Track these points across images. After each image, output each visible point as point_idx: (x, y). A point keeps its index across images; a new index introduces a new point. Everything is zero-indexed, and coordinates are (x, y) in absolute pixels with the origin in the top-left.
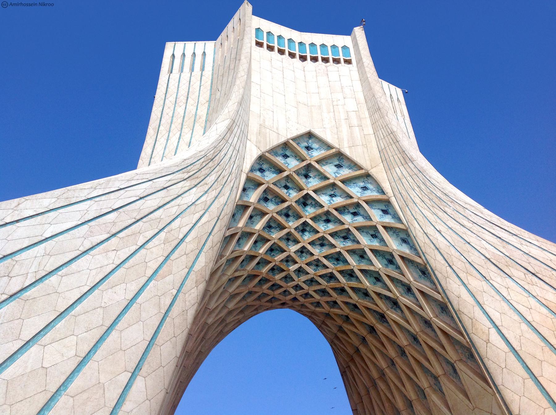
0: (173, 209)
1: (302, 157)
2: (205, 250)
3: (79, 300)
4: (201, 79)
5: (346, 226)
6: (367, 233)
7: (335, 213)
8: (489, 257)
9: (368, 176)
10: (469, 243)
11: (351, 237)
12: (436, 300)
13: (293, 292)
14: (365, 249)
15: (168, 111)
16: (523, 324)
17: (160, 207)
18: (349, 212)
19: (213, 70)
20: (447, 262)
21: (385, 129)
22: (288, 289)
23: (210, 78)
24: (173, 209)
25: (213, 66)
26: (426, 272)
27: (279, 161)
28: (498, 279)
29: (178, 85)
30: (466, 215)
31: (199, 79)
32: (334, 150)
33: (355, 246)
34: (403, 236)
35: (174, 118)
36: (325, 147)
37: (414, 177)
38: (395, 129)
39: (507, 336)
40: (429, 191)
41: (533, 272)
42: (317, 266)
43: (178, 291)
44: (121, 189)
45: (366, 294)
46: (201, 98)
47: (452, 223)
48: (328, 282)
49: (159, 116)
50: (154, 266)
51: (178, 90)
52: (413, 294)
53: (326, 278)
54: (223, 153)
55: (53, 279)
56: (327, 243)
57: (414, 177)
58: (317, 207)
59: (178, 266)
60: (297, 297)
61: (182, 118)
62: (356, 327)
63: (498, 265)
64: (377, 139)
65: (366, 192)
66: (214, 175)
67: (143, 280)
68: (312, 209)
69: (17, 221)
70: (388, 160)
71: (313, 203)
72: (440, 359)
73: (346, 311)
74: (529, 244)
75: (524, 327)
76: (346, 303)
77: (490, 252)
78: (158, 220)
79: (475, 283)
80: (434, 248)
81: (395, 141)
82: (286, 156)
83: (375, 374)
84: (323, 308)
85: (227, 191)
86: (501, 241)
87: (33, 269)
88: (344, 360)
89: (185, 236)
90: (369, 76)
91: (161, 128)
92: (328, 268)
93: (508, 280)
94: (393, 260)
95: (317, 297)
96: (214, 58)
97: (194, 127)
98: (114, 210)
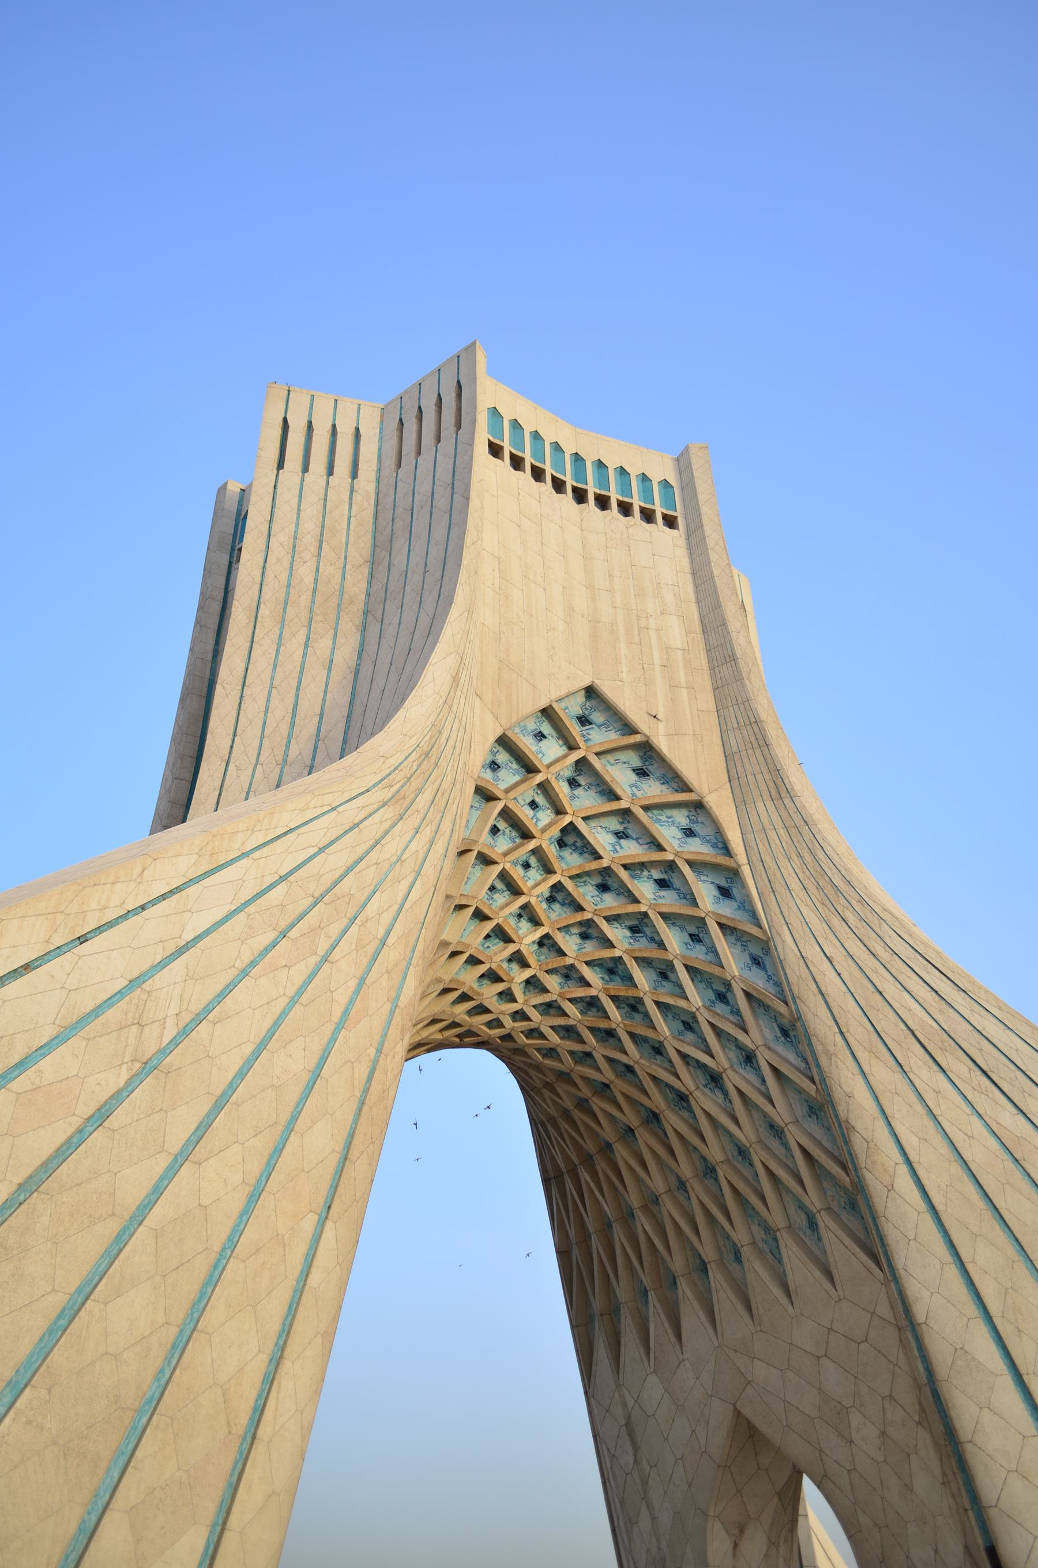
0: (370, 875)
1: (570, 740)
2: (414, 961)
3: (242, 1074)
4: (351, 498)
5: (643, 908)
6: (682, 929)
7: (624, 875)
8: (913, 1027)
9: (699, 806)
10: (880, 993)
11: (648, 931)
12: (801, 1091)
13: (508, 1022)
14: (675, 962)
15: (277, 570)
16: (953, 1163)
17: (350, 869)
18: (650, 877)
19: (378, 480)
20: (837, 1024)
21: (742, 706)
22: (500, 1017)
23: (373, 501)
24: (370, 875)
25: (379, 470)
26: (791, 1033)
28: (923, 1073)
29: (299, 505)
30: (881, 934)
31: (347, 499)
32: (637, 738)
33: (655, 954)
34: (757, 951)
35: (292, 591)
36: (618, 725)
37: (793, 831)
38: (763, 715)
39: (925, 1182)
40: (819, 869)
41: (985, 1068)
42: (567, 977)
44: (291, 831)
45: (658, 1050)
46: (352, 551)
48: (582, 1012)
49: (258, 579)
50: (342, 997)
51: (298, 518)
52: (757, 1069)
53: (580, 1005)
56: (596, 935)
57: (793, 831)
58: (586, 855)
60: (513, 1034)
61: (310, 593)
62: (619, 1108)
63: (926, 1044)
64: (724, 727)
65: (690, 840)
66: (430, 789)
68: (575, 855)
69: (143, 908)
70: (743, 780)
71: (579, 844)
72: (787, 1198)
73: (608, 1074)
74: (984, 1012)
75: (957, 1169)
76: (610, 1060)
77: (917, 1017)
78: (347, 899)
79: (883, 1074)
80: (816, 991)
81: (762, 743)
82: (540, 736)
83: (634, 1199)
84: (561, 1061)
86: (937, 998)
87: (173, 1010)
88: (567, 1158)
89: (388, 933)
90: (716, 572)
91: (264, 611)
92: (589, 985)
93: (941, 1076)
94: (729, 995)
95: (554, 1038)
96: (380, 449)
97: (337, 623)
98: (283, 878)
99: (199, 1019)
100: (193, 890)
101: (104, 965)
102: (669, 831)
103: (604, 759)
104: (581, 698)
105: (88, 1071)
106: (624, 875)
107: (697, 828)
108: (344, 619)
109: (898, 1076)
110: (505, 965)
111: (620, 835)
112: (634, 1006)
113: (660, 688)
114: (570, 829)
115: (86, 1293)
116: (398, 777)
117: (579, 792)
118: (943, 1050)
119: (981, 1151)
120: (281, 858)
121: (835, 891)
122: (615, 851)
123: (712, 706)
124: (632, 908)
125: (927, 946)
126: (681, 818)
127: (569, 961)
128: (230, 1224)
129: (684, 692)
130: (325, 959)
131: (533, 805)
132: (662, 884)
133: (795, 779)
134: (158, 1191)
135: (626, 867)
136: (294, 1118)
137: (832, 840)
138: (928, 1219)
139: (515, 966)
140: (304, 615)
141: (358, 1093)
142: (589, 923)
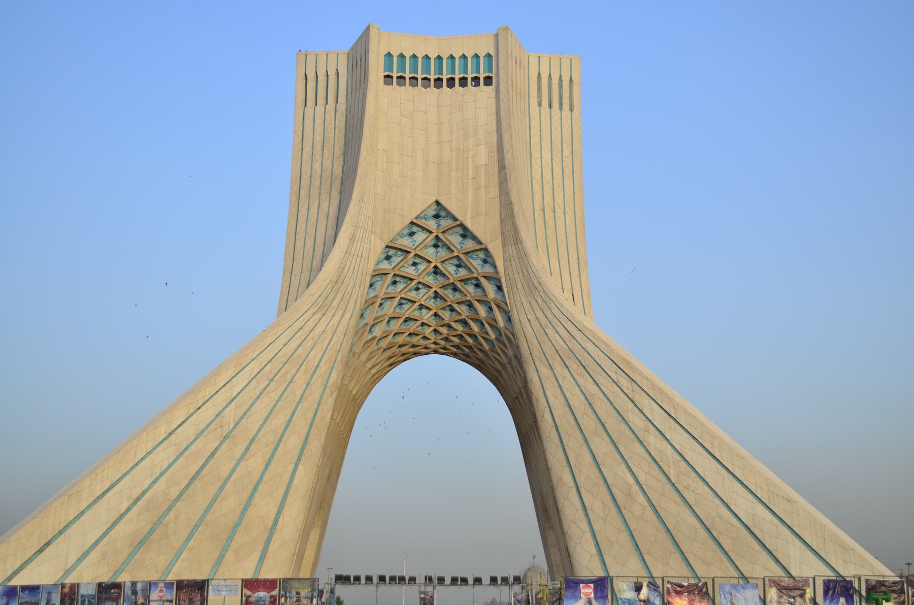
0: (309, 344)
3: (259, 430)
9: (486, 250)
13: (433, 346)
27: (406, 242)
32: (458, 223)
33: (476, 317)
38: (513, 200)
43: (319, 404)
47: (540, 314)
50: (299, 393)
54: (346, 270)
75: (567, 409)
79: (544, 371)
82: (412, 234)
93: (566, 370)
95: (454, 350)
99: (242, 418)
100: (234, 380)
101: (207, 414)
102: (476, 263)
103: (446, 235)
105: (207, 444)
106: (459, 285)
107: (488, 259)
108: (334, 189)
110: (420, 328)
111: (458, 266)
113: (470, 193)
114: (436, 267)
115: (214, 501)
116: (321, 300)
117: (439, 249)
118: (568, 358)
119: (577, 402)
121: (534, 287)
124: (464, 299)
125: (567, 310)
126: (482, 255)
128: (259, 475)
129: (483, 190)
130: (290, 382)
131: (414, 264)
132: (478, 285)
134: (234, 470)
135: (461, 281)
136: (281, 437)
137: (535, 263)
139: (425, 327)
140: (317, 191)
142: (450, 306)
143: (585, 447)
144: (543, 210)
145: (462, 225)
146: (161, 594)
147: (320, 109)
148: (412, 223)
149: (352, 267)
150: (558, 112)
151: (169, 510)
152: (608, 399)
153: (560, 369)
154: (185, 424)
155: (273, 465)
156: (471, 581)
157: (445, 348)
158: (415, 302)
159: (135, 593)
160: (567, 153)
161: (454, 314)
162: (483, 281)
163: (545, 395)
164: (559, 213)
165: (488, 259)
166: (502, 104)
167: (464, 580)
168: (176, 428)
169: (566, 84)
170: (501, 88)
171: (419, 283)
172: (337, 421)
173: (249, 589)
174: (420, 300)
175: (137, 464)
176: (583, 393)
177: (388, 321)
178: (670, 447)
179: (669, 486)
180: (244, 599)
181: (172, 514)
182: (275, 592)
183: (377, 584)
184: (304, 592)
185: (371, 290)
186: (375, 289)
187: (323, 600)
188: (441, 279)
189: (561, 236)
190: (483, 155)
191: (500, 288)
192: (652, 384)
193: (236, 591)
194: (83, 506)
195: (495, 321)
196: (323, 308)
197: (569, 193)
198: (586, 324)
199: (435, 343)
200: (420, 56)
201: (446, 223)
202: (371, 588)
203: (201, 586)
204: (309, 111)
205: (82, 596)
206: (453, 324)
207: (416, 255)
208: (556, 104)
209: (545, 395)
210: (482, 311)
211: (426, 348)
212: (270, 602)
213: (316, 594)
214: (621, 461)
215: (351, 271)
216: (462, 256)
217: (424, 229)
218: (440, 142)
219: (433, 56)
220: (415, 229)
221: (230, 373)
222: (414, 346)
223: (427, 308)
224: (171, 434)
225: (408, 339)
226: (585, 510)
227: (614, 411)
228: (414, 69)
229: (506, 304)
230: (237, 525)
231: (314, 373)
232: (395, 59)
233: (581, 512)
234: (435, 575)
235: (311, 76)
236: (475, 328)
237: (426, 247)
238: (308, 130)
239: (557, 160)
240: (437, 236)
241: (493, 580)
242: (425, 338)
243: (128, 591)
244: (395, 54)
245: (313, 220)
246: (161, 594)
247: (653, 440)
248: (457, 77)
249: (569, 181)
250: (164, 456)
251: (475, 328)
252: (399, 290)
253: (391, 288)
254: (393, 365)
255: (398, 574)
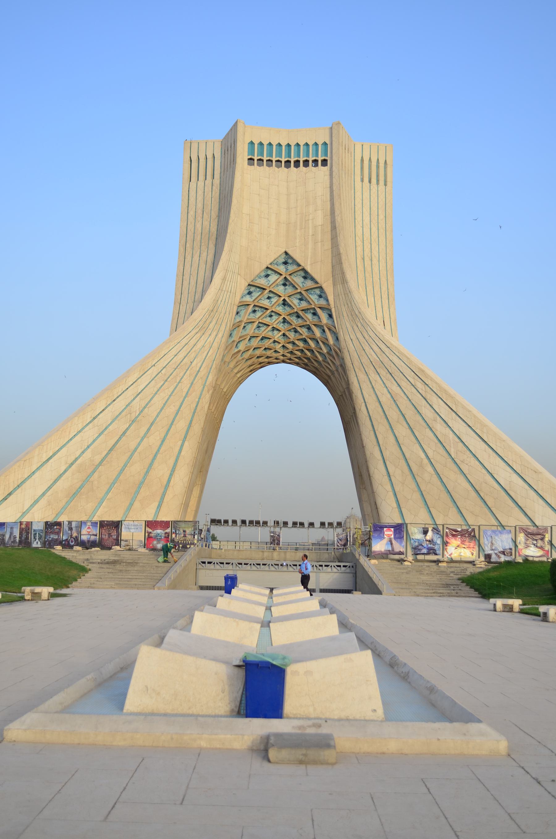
0: (192, 355)
3: (157, 416)
6: (320, 328)
9: (321, 288)
13: (282, 358)
18: (310, 312)
24: (192, 355)
27: (263, 282)
32: (301, 268)
33: (313, 337)
37: (346, 295)
38: (342, 251)
43: (199, 398)
50: (185, 390)
54: (219, 302)
55: (146, 409)
57: (346, 295)
59: (198, 386)
65: (320, 299)
67: (182, 399)
75: (378, 404)
79: (362, 376)
82: (267, 276)
85: (223, 328)
87: (138, 408)
91: (188, 245)
93: (378, 376)
95: (297, 360)
99: (145, 408)
101: (120, 404)
102: (314, 298)
103: (292, 276)
104: (284, 256)
106: (301, 313)
107: (323, 295)
108: (210, 242)
109: (366, 376)
111: (301, 300)
112: (311, 351)
113: (310, 246)
114: (284, 300)
115: (125, 466)
116: (201, 323)
117: (287, 287)
119: (385, 398)
120: (163, 363)
121: (356, 315)
122: (299, 305)
123: (330, 247)
125: (380, 333)
126: (318, 292)
127: (292, 340)
128: (157, 448)
129: (320, 244)
130: (179, 382)
131: (269, 298)
132: (315, 314)
133: (349, 276)
134: (139, 444)
135: (303, 310)
137: (357, 297)
138: (368, 418)
139: (276, 343)
140: (199, 244)
141: (193, 411)
142: (294, 328)
143: (390, 431)
144: (363, 259)
145: (304, 270)
146: (88, 530)
147: (201, 183)
148: (267, 268)
149: (223, 300)
150: (376, 186)
151: (94, 472)
152: (408, 397)
153: (373, 376)
154: (104, 412)
155: (167, 441)
156: (306, 525)
157: (290, 359)
158: (269, 325)
159: (71, 529)
160: (382, 217)
161: (297, 334)
162: (318, 310)
163: (362, 393)
164: (375, 261)
165: (322, 295)
166: (334, 181)
167: (302, 524)
168: (98, 415)
169: (382, 165)
170: (334, 168)
171: (272, 311)
172: (213, 410)
173: (150, 528)
174: (272, 324)
175: (71, 439)
176: (389, 393)
177: (250, 339)
178: (451, 432)
179: (450, 460)
180: (147, 534)
181: (96, 475)
182: (169, 530)
183: (241, 526)
184: (189, 531)
185: (237, 317)
186: (240, 316)
187: (202, 536)
188: (288, 309)
189: (376, 278)
190: (320, 218)
191: (330, 316)
192: (440, 386)
193: (141, 529)
194: (34, 468)
195: (327, 340)
196: (203, 329)
197: (382, 247)
198: (392, 342)
199: (283, 355)
200: (274, 144)
201: (292, 268)
202: (236, 529)
203: (117, 525)
204: (193, 184)
205: (34, 530)
206: (297, 342)
207: (270, 291)
208: (374, 180)
209: (362, 393)
210: (317, 333)
211: (276, 359)
212: (165, 537)
213: (197, 532)
214: (416, 442)
215: (223, 303)
216: (303, 293)
217: (276, 272)
218: (288, 208)
219: (284, 144)
220: (269, 272)
221: (136, 375)
222: (268, 357)
223: (278, 330)
224: (94, 418)
225: (264, 352)
226: (389, 476)
227: (412, 406)
228: (270, 154)
229: (335, 328)
230: (142, 483)
231: (196, 376)
232: (256, 146)
233: (386, 477)
234: (281, 520)
235: (194, 159)
236: (312, 344)
237: (277, 285)
238: (192, 199)
239: (374, 222)
240: (285, 278)
241: (323, 524)
242: (276, 351)
243: (66, 527)
244: (256, 143)
245: (195, 265)
246: (88, 530)
247: (439, 428)
248: (302, 159)
249: (382, 238)
250: (90, 433)
251: (312, 344)
252: (257, 317)
253: (252, 315)
254: (253, 371)
255: (255, 519)
